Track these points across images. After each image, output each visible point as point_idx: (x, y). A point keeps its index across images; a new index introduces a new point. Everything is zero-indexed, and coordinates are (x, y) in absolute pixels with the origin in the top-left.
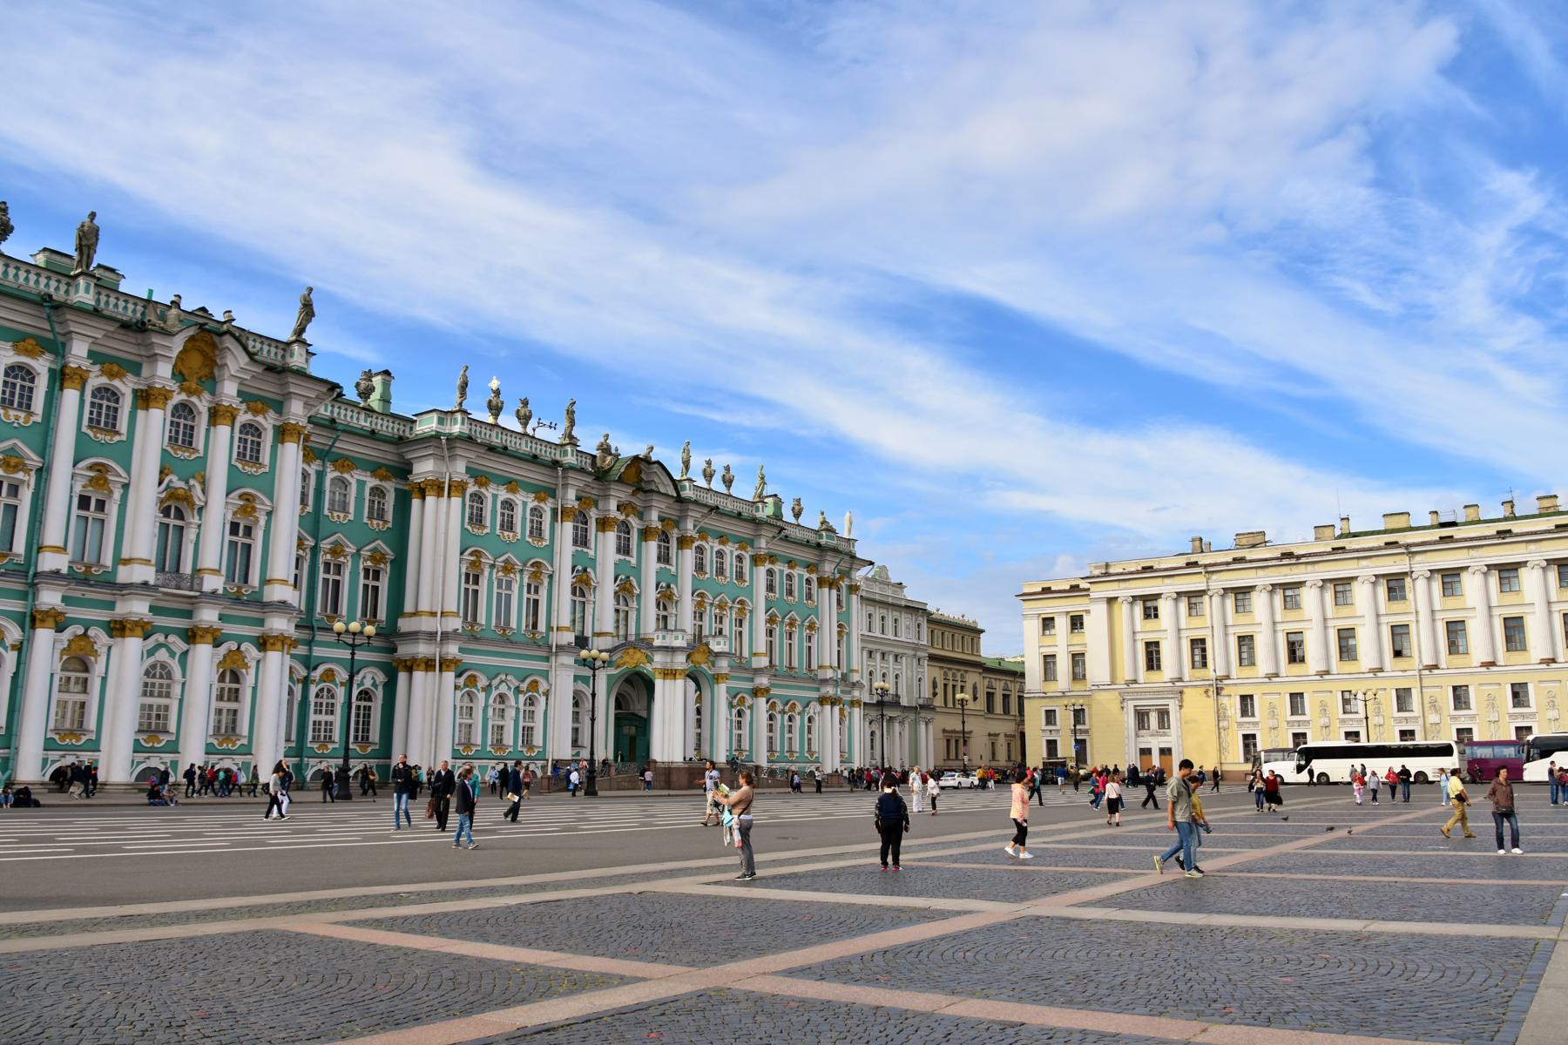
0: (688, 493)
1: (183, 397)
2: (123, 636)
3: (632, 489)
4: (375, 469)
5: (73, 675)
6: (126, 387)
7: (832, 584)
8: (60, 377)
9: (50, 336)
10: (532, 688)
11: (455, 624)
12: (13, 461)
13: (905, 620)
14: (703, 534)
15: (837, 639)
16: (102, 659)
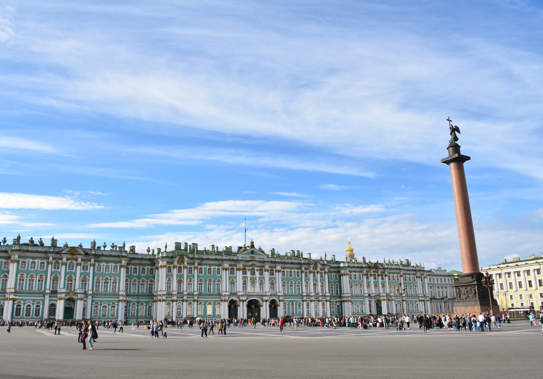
0: (386, 267)
3: (374, 269)
4: (335, 272)
6: (308, 271)
7: (419, 277)
8: (302, 272)
10: (362, 303)
11: (350, 295)
13: (447, 278)
14: (389, 273)
15: (422, 288)
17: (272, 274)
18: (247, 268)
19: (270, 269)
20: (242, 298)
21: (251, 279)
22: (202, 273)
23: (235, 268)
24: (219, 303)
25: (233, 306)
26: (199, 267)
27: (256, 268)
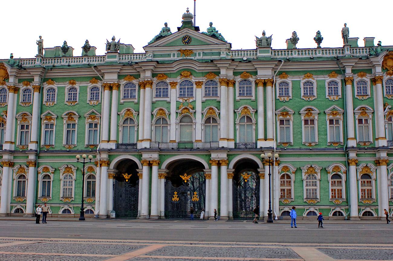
1: (389, 76)
2: (380, 165)
5: (366, 180)
6: (367, 79)
8: (344, 82)
9: (339, 69)
12: (335, 112)
16: (375, 174)
17: (246, 92)
18: (168, 81)
19: (238, 79)
20: (145, 156)
21: (178, 108)
22: (53, 100)
23: (135, 81)
24: (91, 169)
25: (126, 176)
26: (46, 86)
27: (193, 80)
